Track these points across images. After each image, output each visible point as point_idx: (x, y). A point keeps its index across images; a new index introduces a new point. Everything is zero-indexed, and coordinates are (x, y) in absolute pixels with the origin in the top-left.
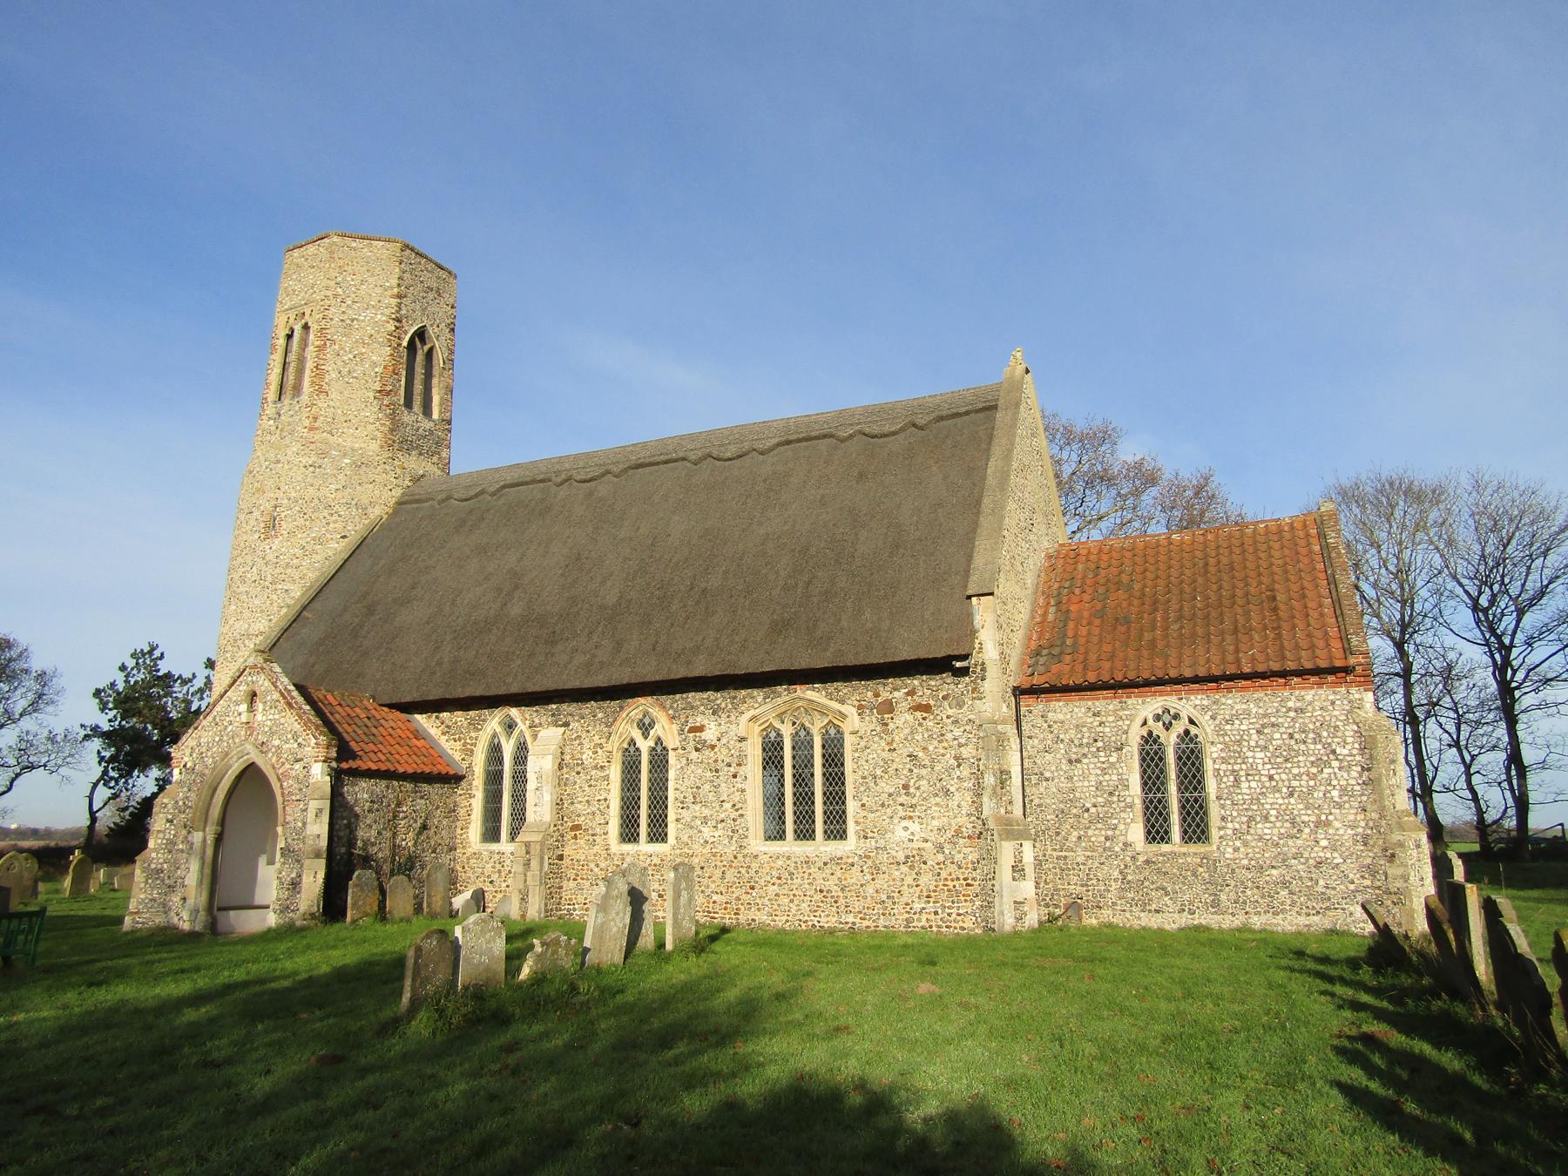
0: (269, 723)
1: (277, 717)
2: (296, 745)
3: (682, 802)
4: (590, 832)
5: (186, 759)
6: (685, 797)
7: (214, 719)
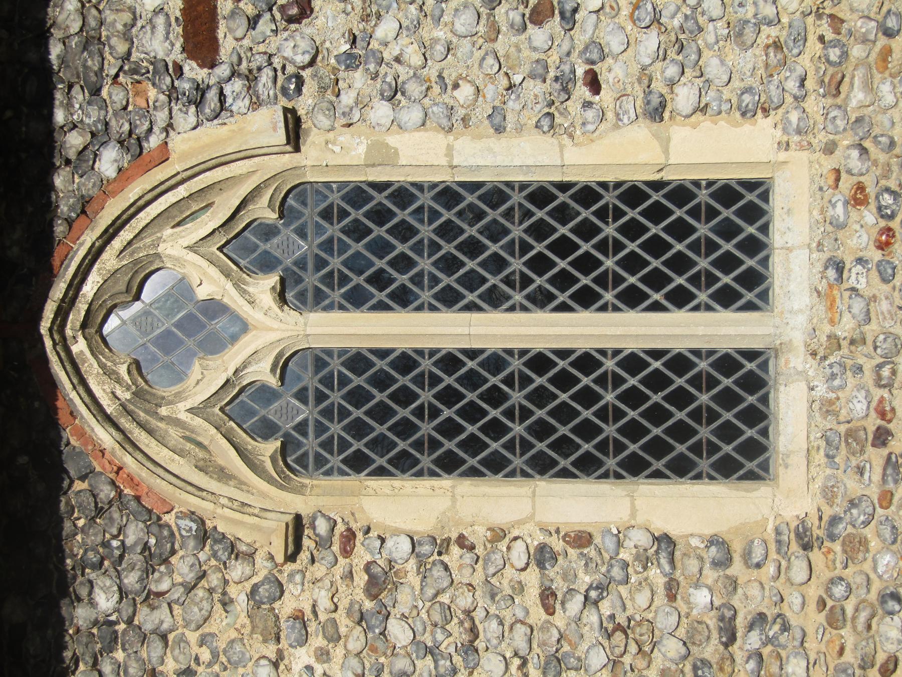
3: (565, 85)
4: (711, 650)
6: (539, 73)
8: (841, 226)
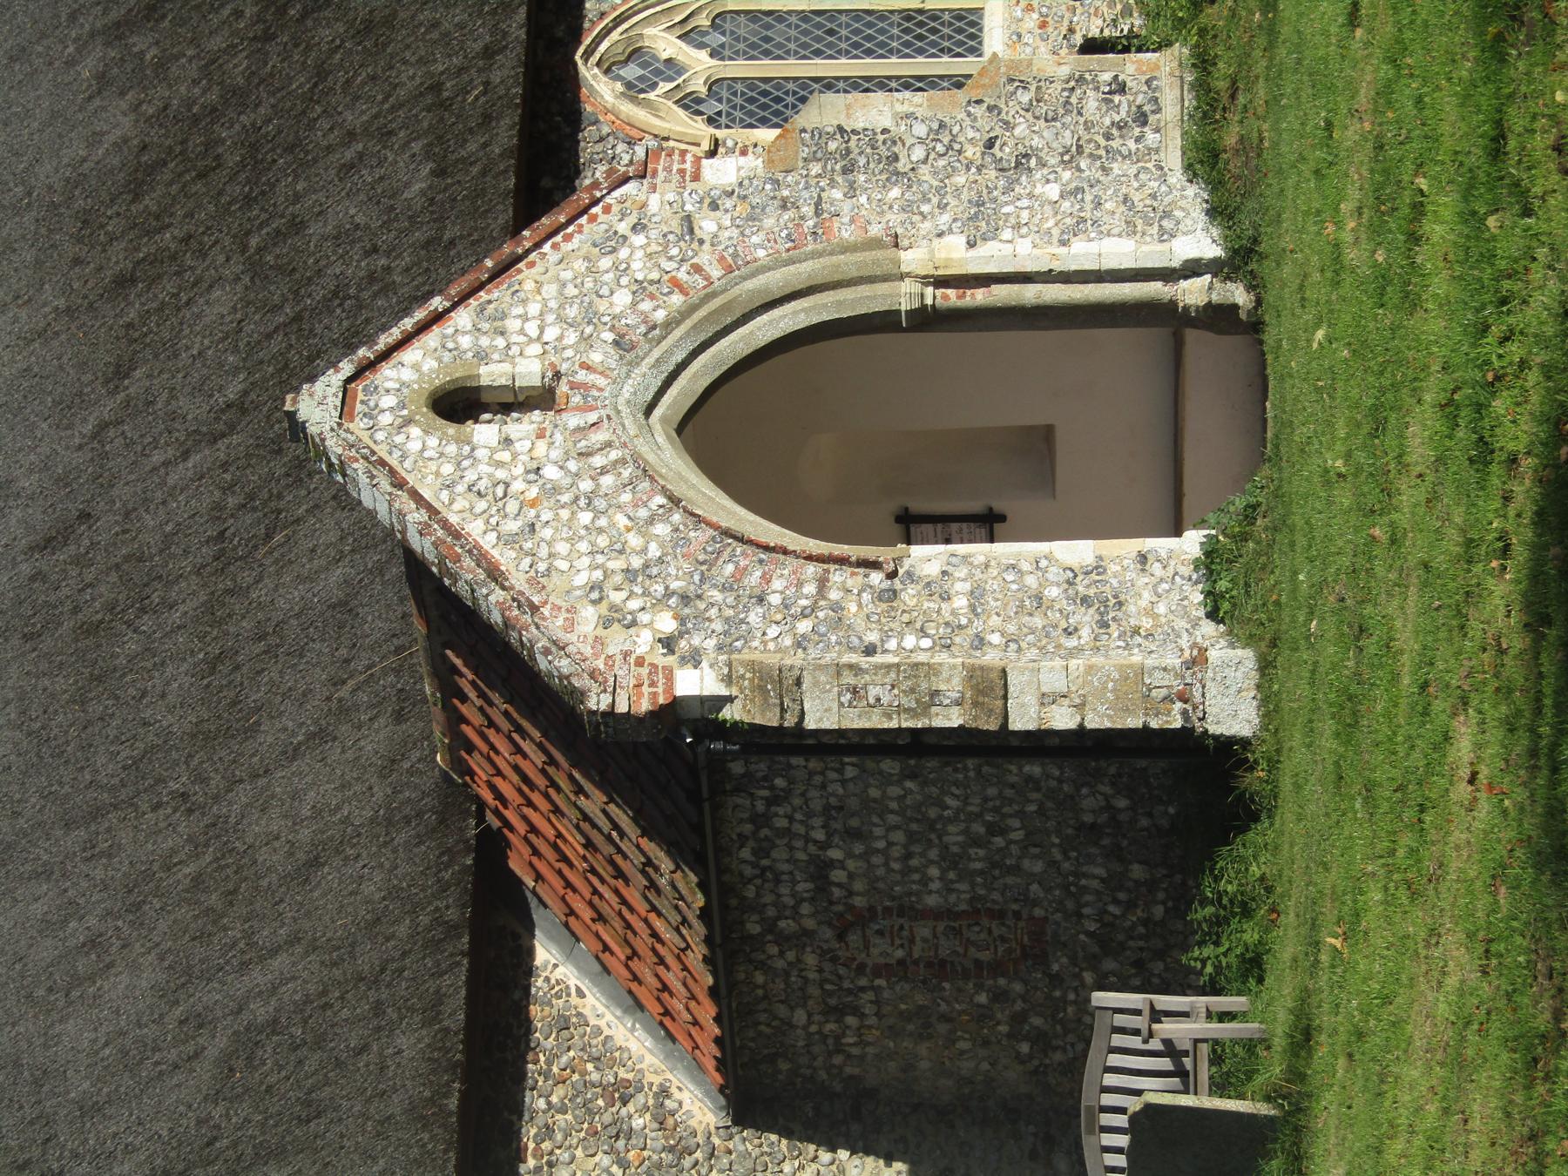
0: (551, 334)
1: (534, 309)
2: (638, 240)
5: (644, 642)
7: (510, 541)
8: (1021, 20)
